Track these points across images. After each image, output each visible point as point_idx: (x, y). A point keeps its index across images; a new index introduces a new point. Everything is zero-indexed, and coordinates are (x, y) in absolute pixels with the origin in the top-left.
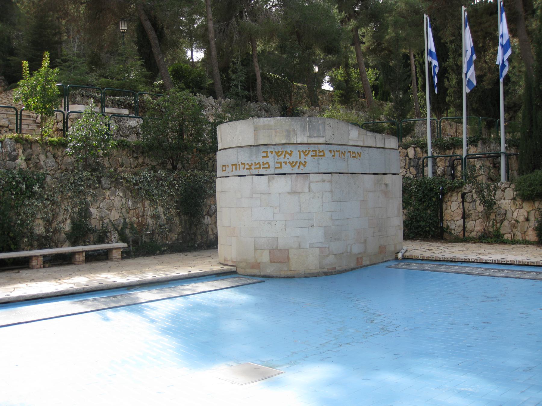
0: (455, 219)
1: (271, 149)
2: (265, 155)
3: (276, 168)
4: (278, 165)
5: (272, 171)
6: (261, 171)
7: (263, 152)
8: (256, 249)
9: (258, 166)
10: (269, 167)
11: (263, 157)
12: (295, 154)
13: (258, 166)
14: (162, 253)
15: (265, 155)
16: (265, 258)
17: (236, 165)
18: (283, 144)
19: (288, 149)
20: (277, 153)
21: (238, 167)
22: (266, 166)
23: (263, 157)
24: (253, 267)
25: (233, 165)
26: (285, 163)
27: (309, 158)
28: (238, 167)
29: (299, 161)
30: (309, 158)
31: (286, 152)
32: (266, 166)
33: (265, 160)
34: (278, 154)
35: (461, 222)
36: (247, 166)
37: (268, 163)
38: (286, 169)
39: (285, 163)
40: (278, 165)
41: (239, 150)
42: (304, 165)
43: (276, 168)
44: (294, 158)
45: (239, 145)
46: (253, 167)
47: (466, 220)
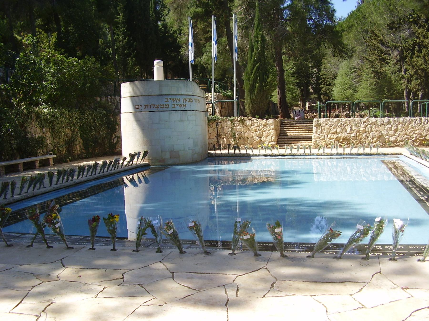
0: (212, 138)
1: (169, 97)
2: (167, 100)
3: (173, 107)
4: (174, 106)
5: (170, 109)
6: (165, 109)
7: (166, 99)
8: (162, 152)
9: (163, 106)
10: (169, 107)
11: (165, 102)
12: (181, 100)
13: (163, 106)
14: (82, 159)
15: (167, 100)
16: (167, 156)
17: (148, 105)
18: (175, 95)
19: (178, 97)
20: (173, 99)
21: (149, 106)
22: (167, 106)
23: (165, 102)
24: (160, 161)
25: (145, 105)
26: (177, 105)
27: (187, 103)
28: (149, 106)
29: (183, 104)
30: (187, 103)
31: (177, 99)
32: (167, 106)
33: (167, 103)
34: (173, 100)
35: (216, 140)
36: (156, 106)
37: (168, 105)
38: (177, 108)
39: (177, 105)
40: (174, 106)
41: (150, 97)
42: (185, 107)
43: (173, 107)
44: (181, 102)
45: (150, 94)
46: (159, 107)
47: (219, 138)
